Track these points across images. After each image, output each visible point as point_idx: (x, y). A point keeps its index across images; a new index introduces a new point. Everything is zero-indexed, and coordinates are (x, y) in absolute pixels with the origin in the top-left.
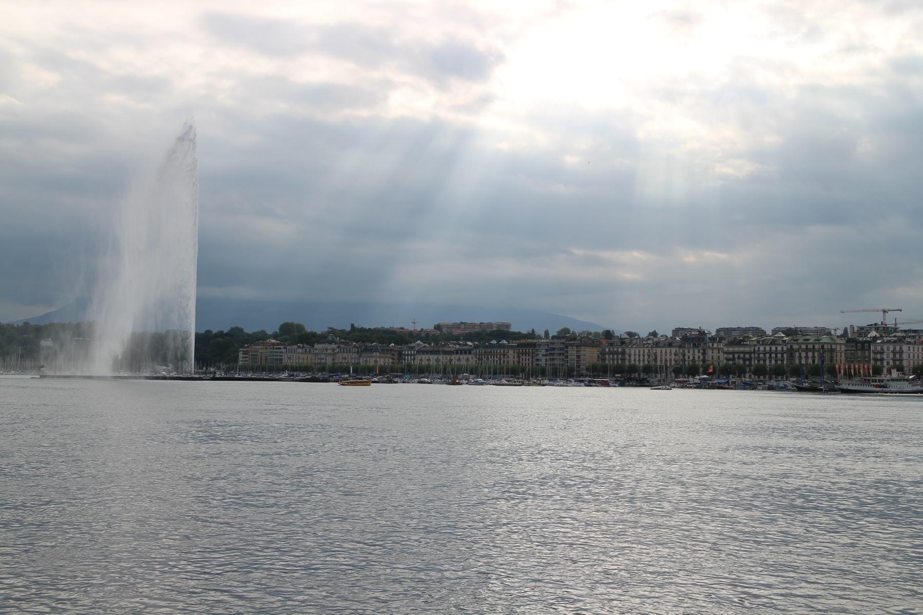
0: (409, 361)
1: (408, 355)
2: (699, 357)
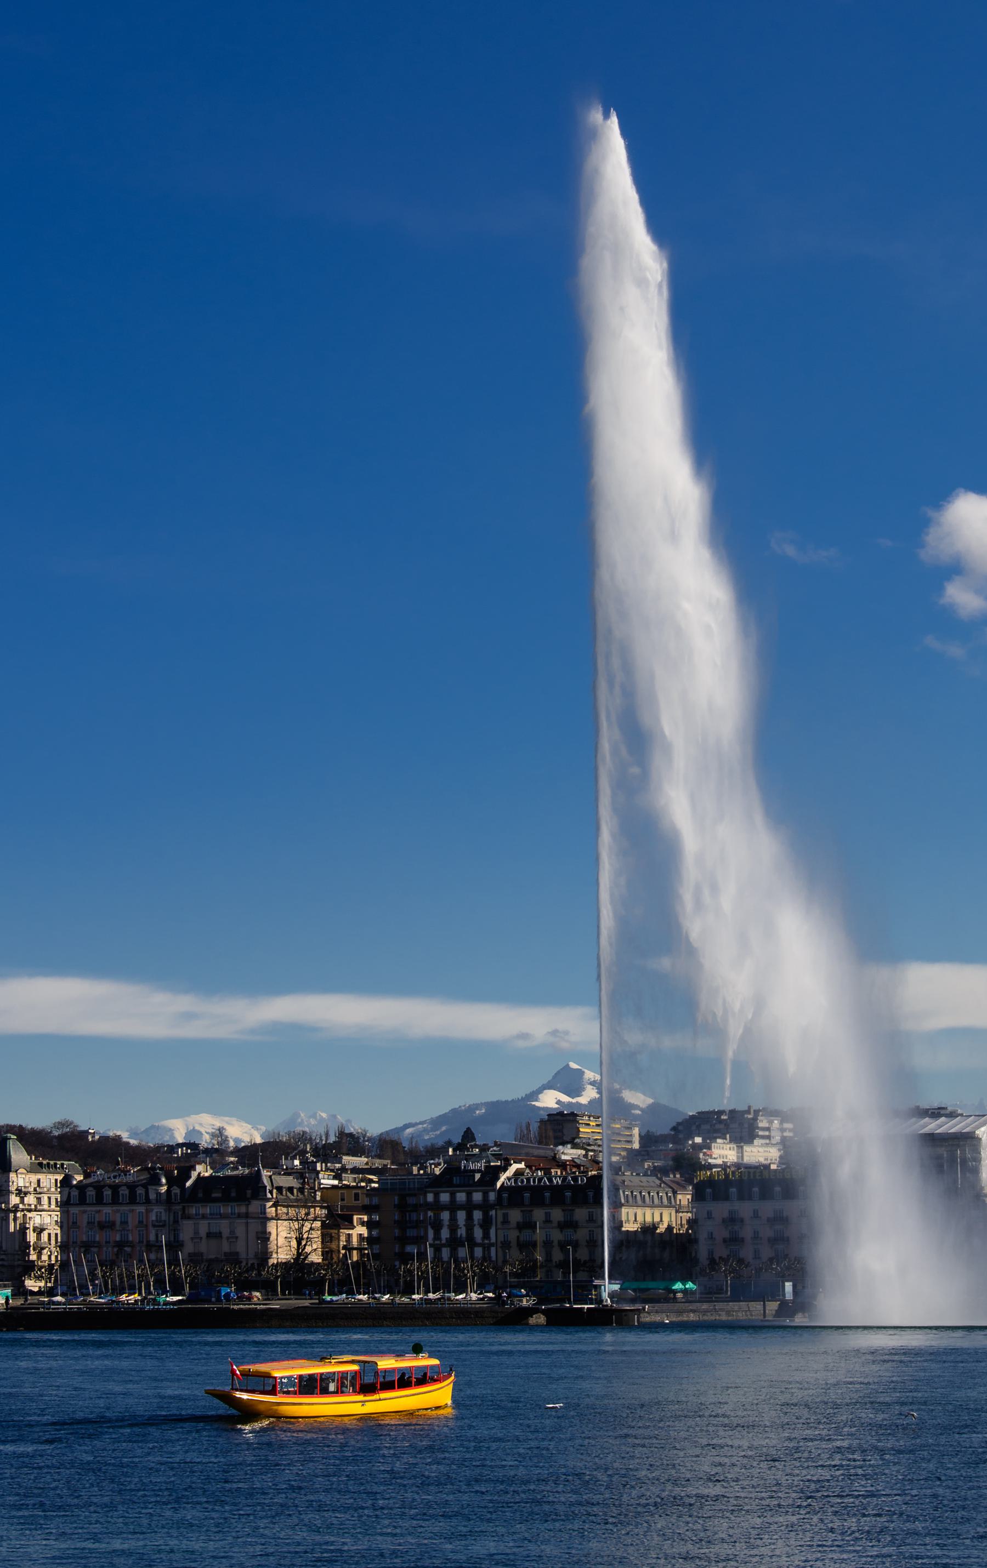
0: (462, 1232)
1: (453, 1207)
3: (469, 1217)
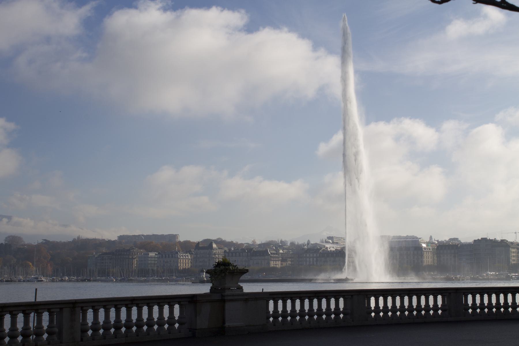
0: (312, 263)
3: (313, 260)
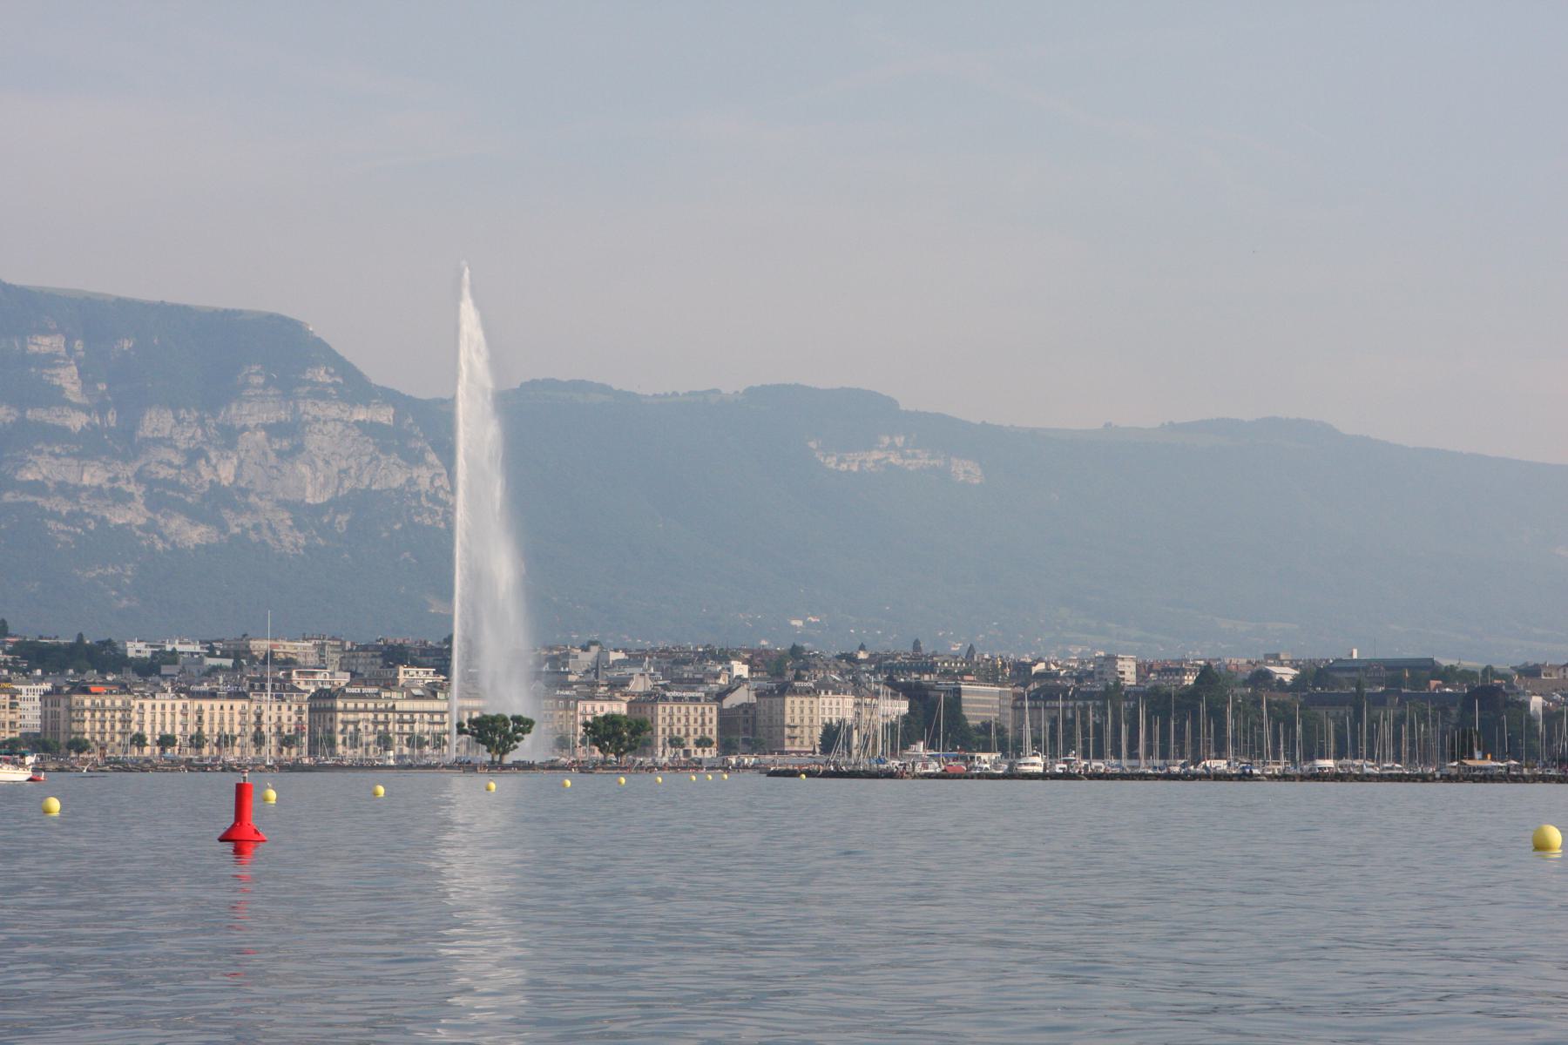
2: (290, 720)
